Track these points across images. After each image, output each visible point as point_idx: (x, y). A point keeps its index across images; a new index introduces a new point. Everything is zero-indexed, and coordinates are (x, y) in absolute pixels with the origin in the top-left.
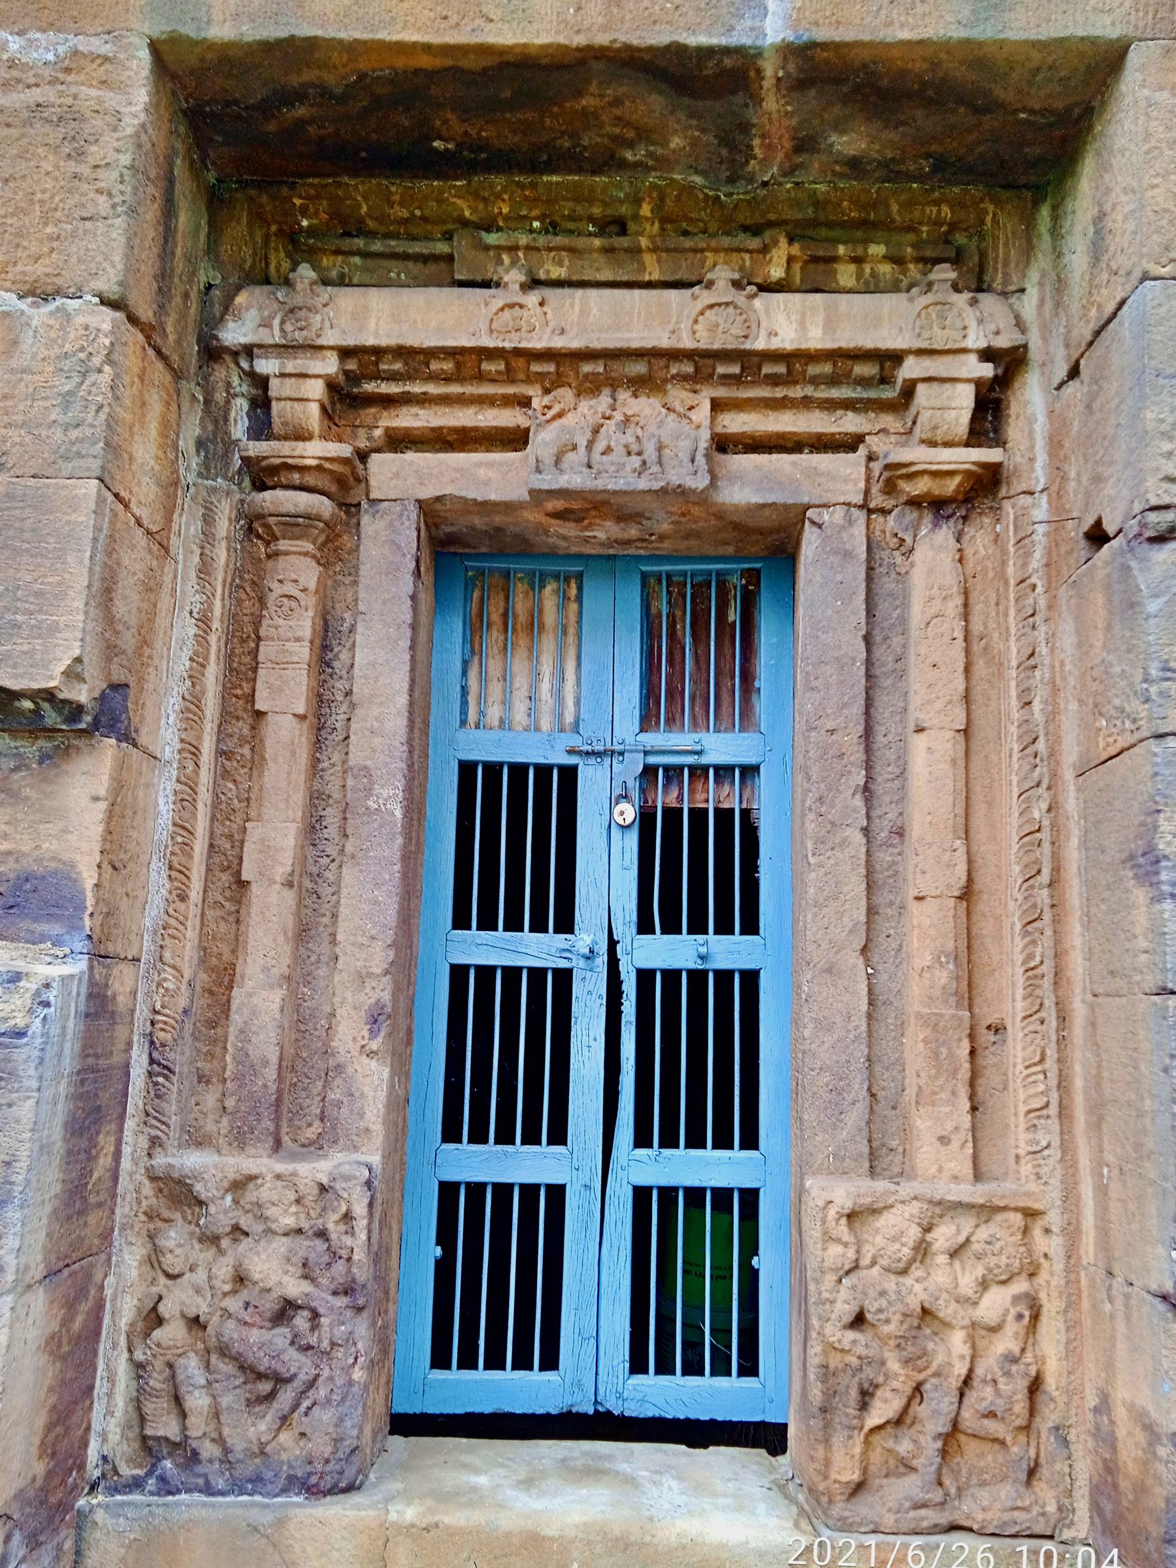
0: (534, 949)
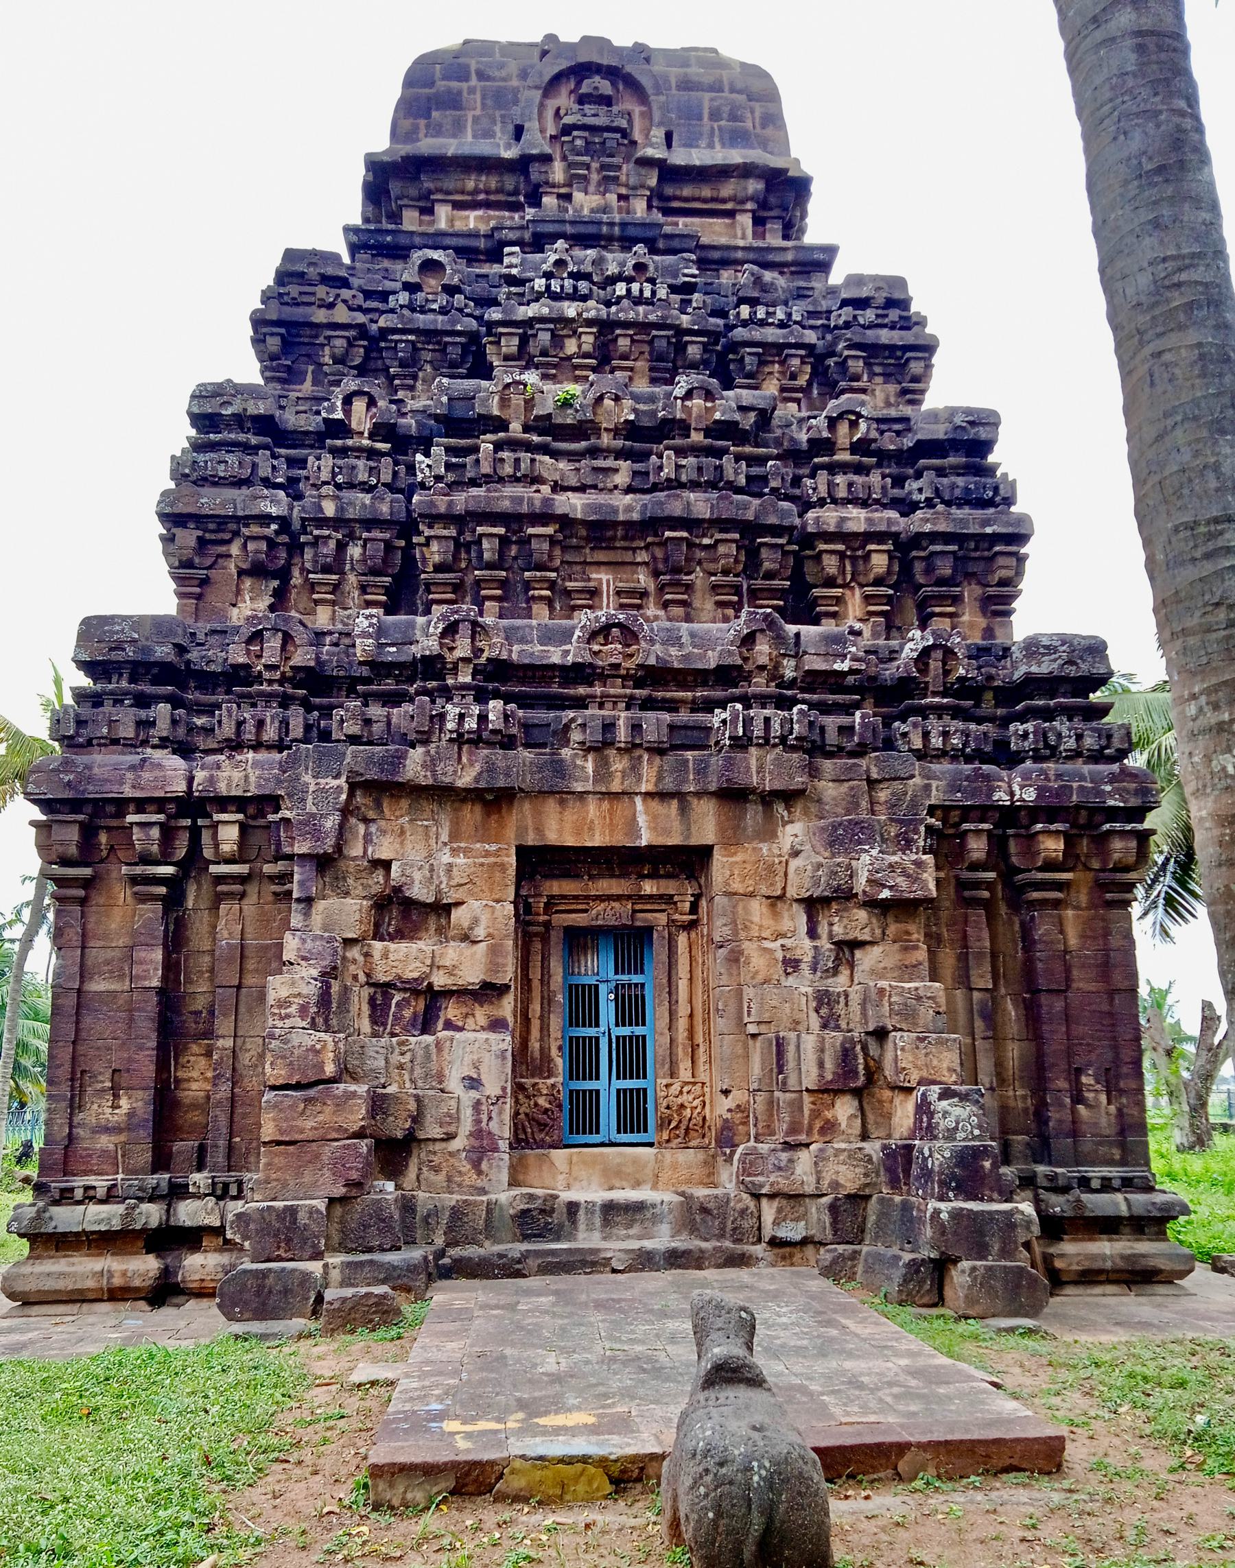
0: (590, 1032)
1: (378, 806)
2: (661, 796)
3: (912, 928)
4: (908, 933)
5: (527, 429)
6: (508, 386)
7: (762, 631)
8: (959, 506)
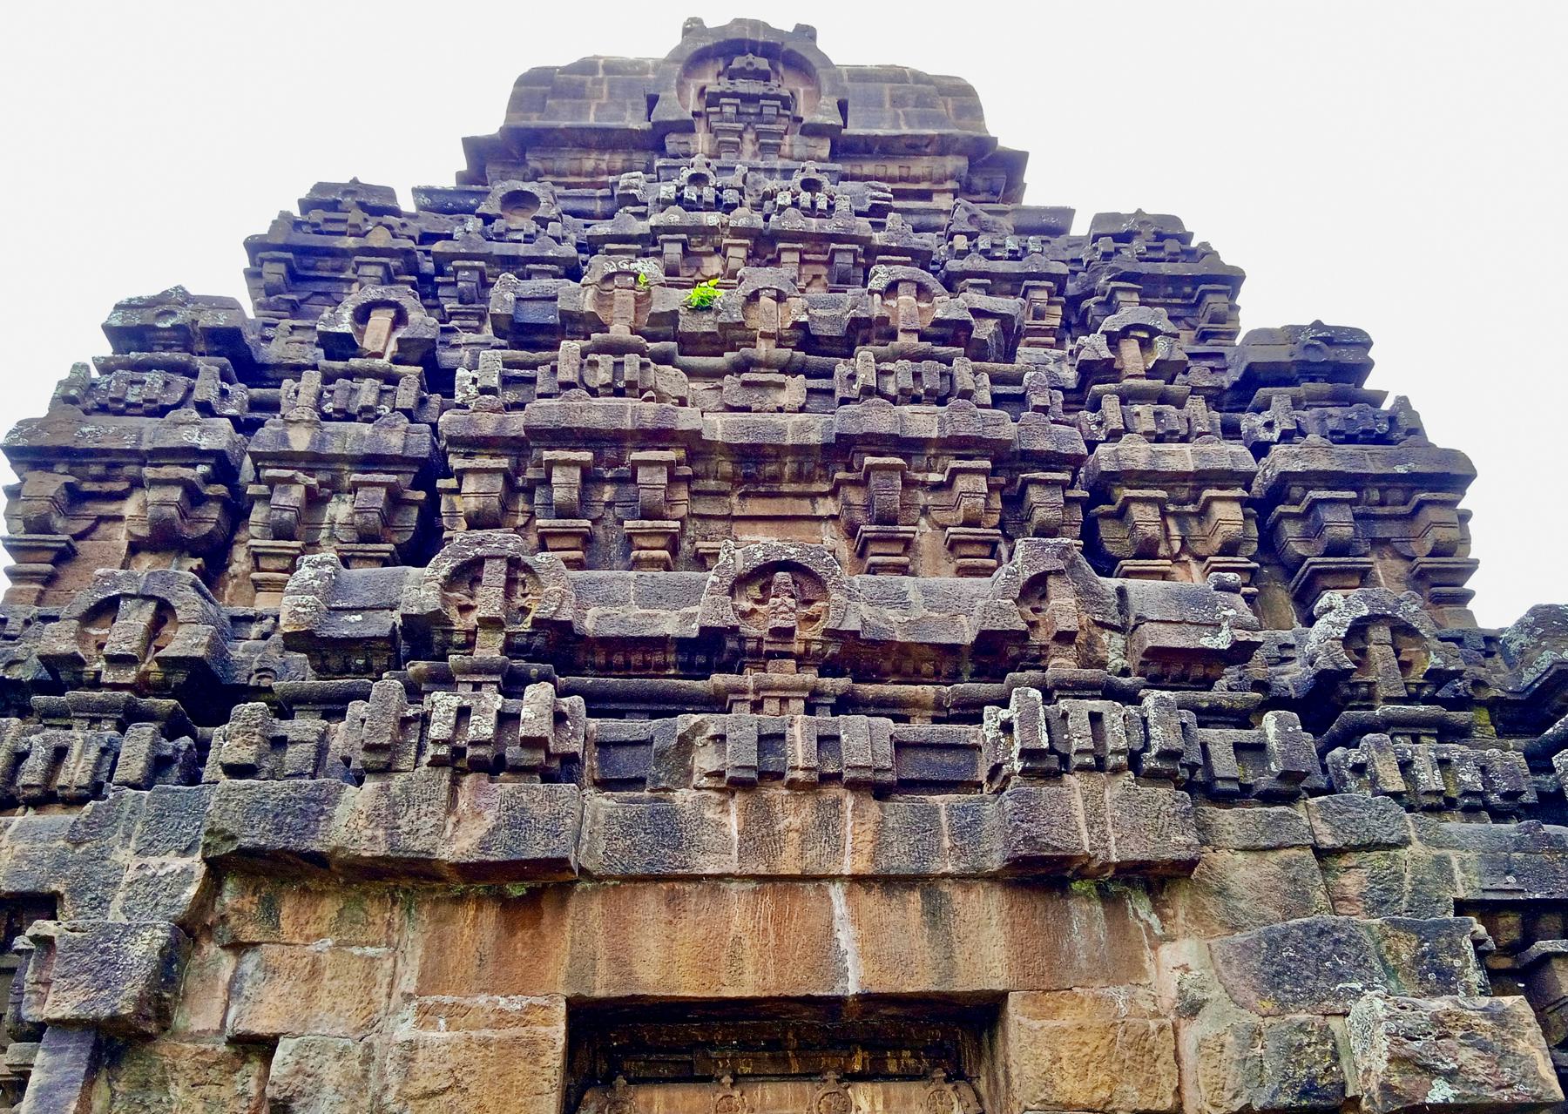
1: (270, 910)
6: (609, 277)
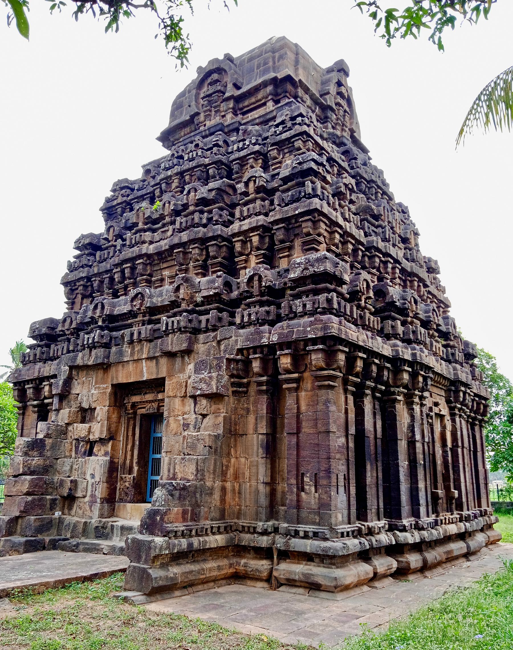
1: (78, 373)
2: (149, 359)
3: (221, 406)
4: (219, 409)
5: (146, 224)
7: (182, 284)
8: (291, 204)
